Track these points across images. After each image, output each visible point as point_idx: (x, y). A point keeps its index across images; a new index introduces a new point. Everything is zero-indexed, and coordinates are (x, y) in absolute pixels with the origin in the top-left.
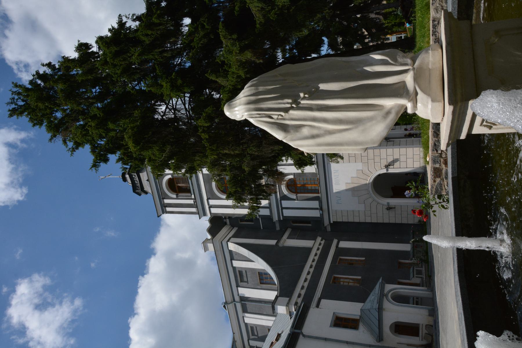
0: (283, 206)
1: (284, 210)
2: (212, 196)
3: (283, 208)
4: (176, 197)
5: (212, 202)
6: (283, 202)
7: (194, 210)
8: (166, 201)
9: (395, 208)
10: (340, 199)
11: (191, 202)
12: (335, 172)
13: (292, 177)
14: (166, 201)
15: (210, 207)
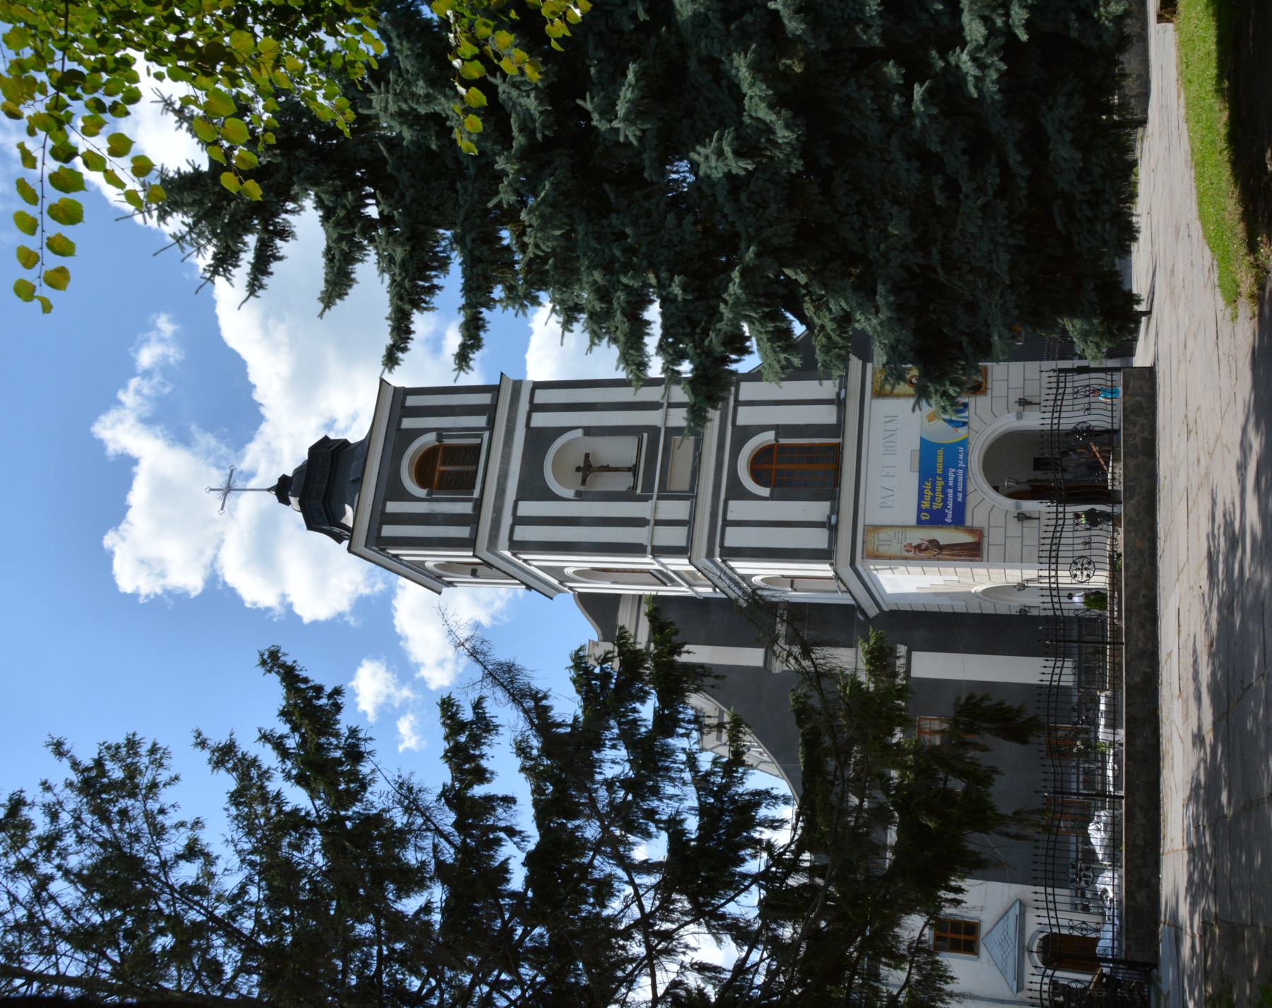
0: (730, 517)
1: (730, 531)
2: (533, 487)
3: (727, 523)
4: (428, 495)
5: (527, 509)
6: (733, 504)
7: (463, 532)
8: (392, 507)
9: (1039, 519)
10: (891, 493)
11: (466, 508)
12: (886, 420)
13: (768, 437)
14: (392, 507)
15: (518, 521)
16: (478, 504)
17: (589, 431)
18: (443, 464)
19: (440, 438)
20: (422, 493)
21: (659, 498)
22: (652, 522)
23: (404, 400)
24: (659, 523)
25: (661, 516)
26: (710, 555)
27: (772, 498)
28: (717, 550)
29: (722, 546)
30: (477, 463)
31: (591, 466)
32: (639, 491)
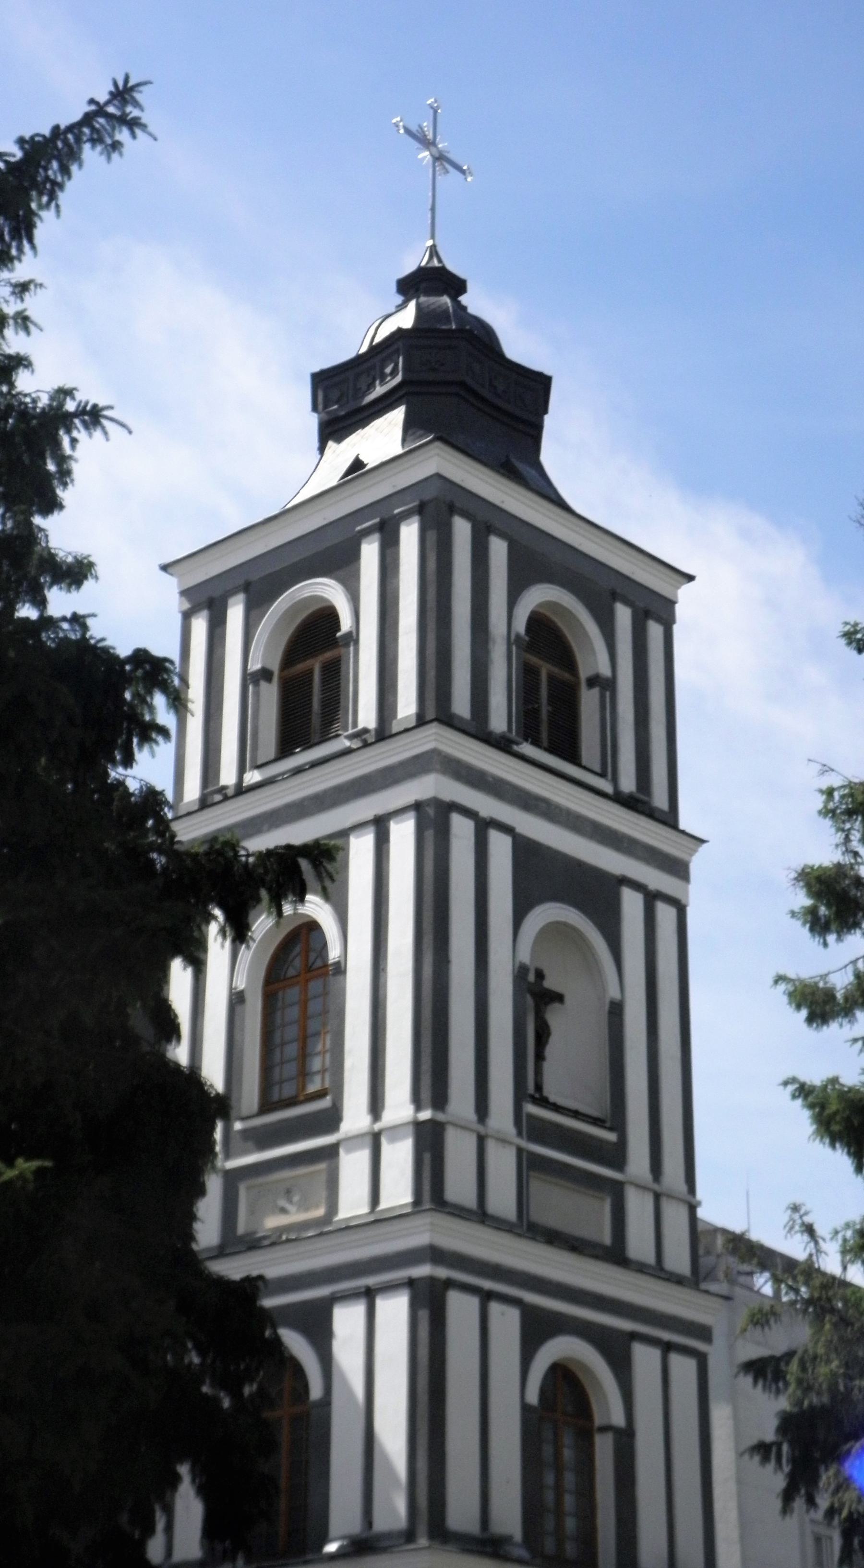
16: (503, 744)
17: (616, 1010)
18: (551, 678)
19: (594, 681)
20: (520, 625)
21: (520, 1151)
22: (481, 1129)
23: (659, 620)
24: (481, 1141)
25: (491, 1147)
26: (436, 1254)
27: (526, 1408)
28: (442, 1273)
29: (449, 1284)
30: (552, 750)
31: (547, 1004)
32: (531, 1108)
